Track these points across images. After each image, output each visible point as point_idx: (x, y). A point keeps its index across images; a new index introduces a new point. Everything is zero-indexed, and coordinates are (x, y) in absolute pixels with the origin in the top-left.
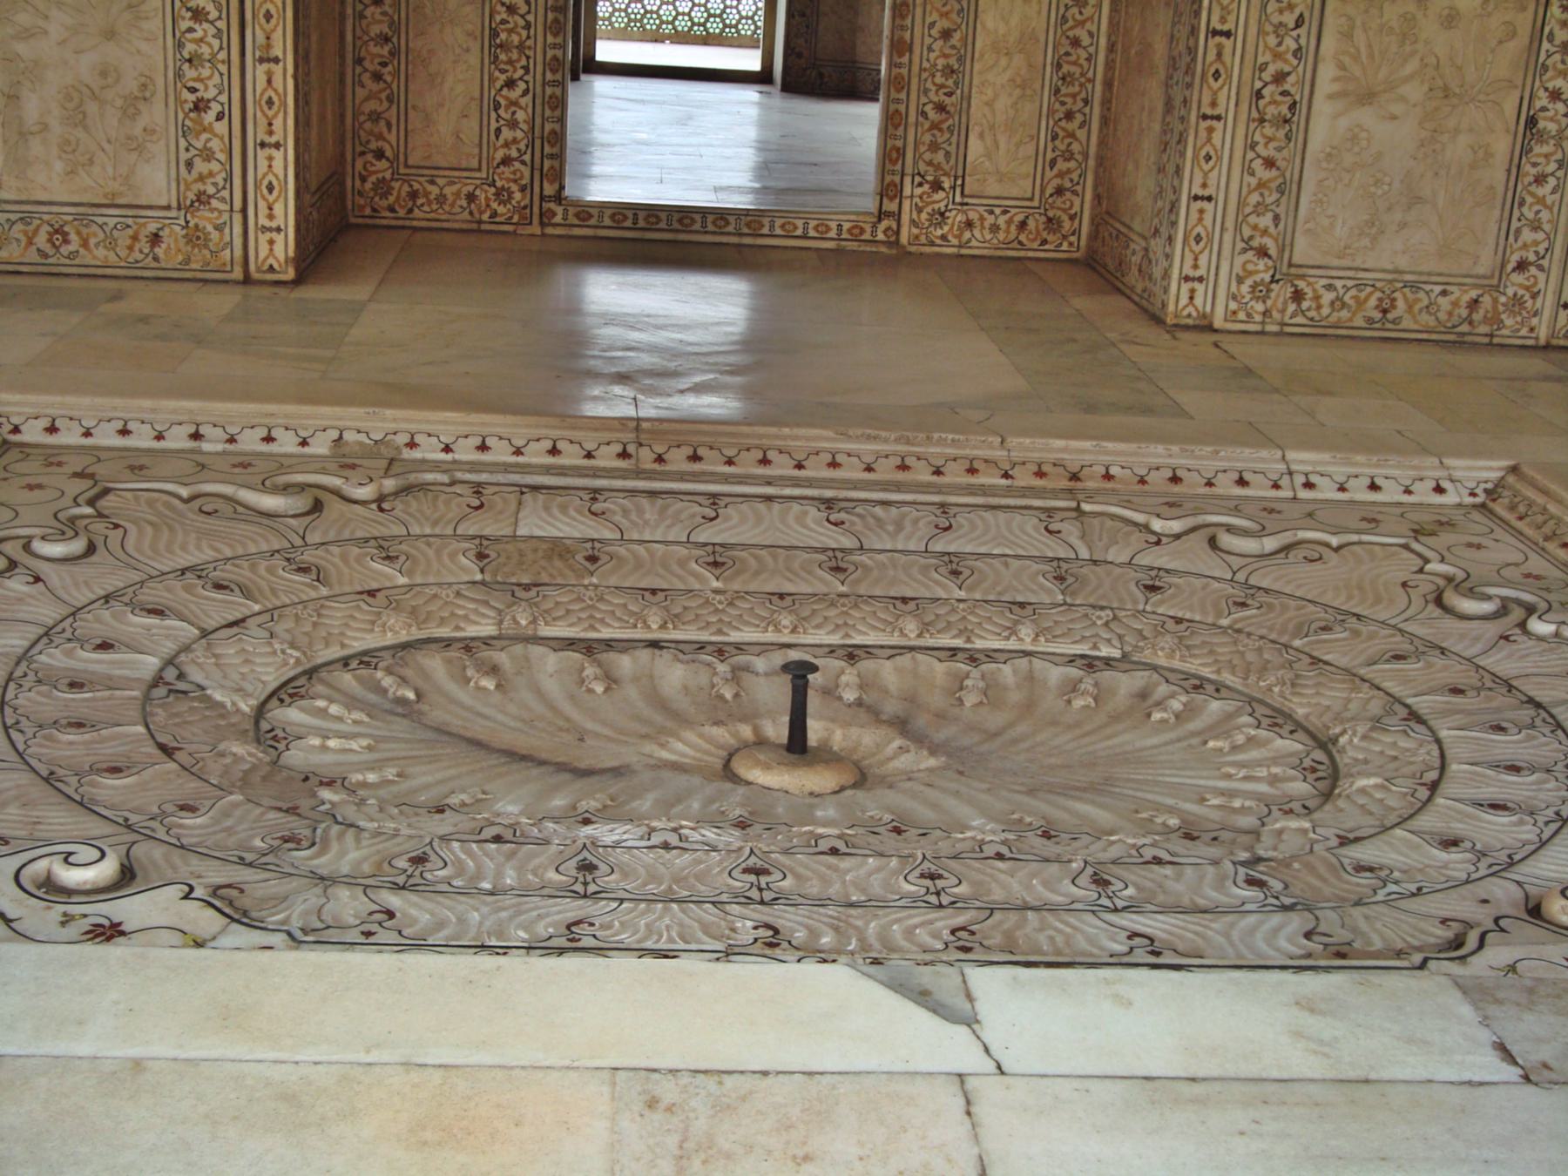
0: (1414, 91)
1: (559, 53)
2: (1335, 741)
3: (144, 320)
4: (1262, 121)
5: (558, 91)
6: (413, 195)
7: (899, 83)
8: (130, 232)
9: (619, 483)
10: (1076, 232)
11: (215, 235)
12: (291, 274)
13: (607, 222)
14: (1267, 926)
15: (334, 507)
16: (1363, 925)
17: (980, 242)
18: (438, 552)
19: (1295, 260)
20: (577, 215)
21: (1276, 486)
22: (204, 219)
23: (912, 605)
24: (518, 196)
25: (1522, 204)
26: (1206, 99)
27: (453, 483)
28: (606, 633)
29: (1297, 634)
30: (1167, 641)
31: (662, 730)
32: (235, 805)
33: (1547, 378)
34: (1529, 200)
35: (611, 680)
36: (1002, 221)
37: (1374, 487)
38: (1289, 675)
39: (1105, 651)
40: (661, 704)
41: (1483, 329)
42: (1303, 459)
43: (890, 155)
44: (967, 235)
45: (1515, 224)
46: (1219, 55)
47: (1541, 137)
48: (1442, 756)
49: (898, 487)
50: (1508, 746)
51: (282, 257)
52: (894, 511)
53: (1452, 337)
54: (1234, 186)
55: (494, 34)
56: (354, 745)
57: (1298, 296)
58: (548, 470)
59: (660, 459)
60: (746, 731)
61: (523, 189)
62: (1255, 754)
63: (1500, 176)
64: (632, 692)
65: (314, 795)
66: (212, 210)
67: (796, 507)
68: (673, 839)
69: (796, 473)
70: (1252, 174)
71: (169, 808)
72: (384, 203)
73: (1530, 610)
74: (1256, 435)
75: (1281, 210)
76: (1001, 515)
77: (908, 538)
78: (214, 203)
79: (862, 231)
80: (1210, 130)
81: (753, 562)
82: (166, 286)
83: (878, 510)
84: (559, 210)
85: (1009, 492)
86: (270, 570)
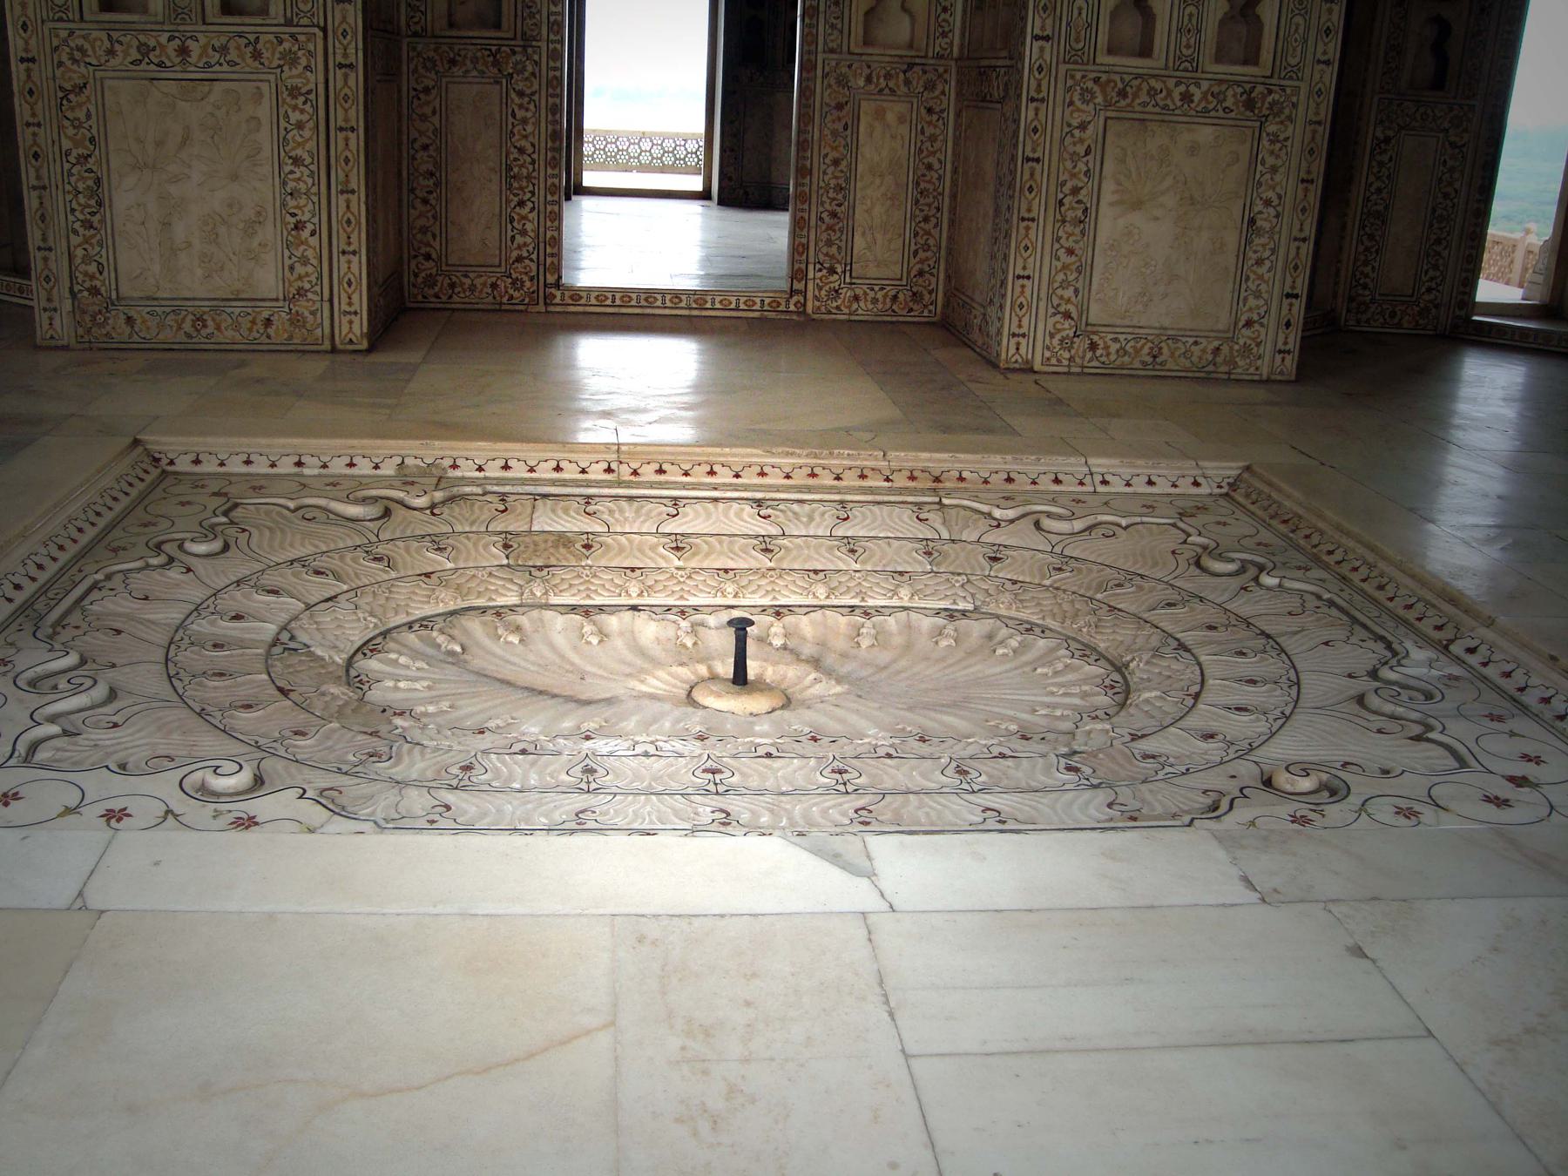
1: (556, 181)
2: (1127, 666)
3: (260, 381)
4: (1064, 221)
5: (556, 208)
7: (803, 198)
9: (606, 491)
10: (934, 303)
12: (365, 345)
13: (593, 302)
14: (1080, 801)
15: (399, 513)
16: (1148, 797)
17: (864, 310)
18: (475, 545)
20: (571, 297)
21: (1081, 484)
22: (303, 307)
23: (821, 575)
24: (528, 284)
25: (1248, 279)
26: (1024, 206)
27: (484, 494)
28: (598, 601)
29: (1099, 589)
30: (1007, 597)
31: (642, 671)
32: (333, 731)
34: (1252, 276)
35: (603, 635)
36: (880, 295)
37: (1150, 483)
38: (1093, 620)
39: (961, 606)
40: (641, 652)
41: (1223, 369)
42: (1100, 464)
43: (798, 249)
44: (855, 306)
46: (1032, 175)
47: (1260, 232)
48: (1202, 674)
49: (810, 489)
50: (1247, 666)
52: (806, 507)
54: (1046, 270)
56: (418, 686)
57: (1093, 346)
58: (553, 483)
59: (635, 473)
60: (703, 670)
61: (532, 279)
62: (1070, 677)
64: (619, 643)
65: (390, 722)
67: (735, 505)
68: (652, 750)
69: (735, 481)
70: (1058, 259)
71: (287, 733)
72: (431, 292)
73: (1261, 568)
74: (1067, 447)
76: (885, 508)
77: (818, 526)
78: (310, 295)
79: (779, 304)
80: (1028, 228)
81: (705, 547)
82: (274, 356)
83: (795, 507)
84: (558, 294)
85: (890, 491)
86: (354, 560)
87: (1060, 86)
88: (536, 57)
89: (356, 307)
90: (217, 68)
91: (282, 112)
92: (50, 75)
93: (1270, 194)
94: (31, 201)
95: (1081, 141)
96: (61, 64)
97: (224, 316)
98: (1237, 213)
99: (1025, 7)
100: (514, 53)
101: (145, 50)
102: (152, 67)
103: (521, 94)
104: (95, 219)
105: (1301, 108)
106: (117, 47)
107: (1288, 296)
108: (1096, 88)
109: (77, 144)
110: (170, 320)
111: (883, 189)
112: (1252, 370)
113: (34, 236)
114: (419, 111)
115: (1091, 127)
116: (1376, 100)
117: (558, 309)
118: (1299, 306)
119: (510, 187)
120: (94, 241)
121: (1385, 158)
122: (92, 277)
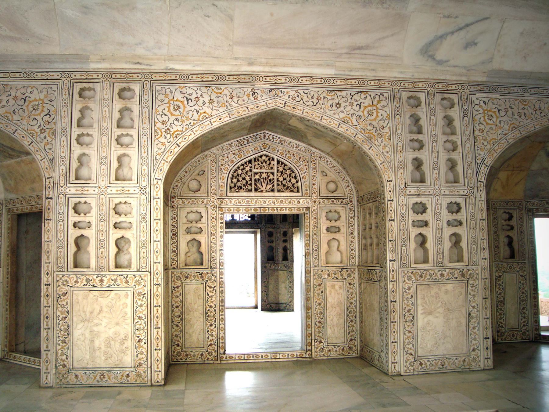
0: (441, 310)
3: (129, 401)
4: (406, 322)
6: (187, 355)
8: (121, 374)
10: (357, 350)
11: (143, 374)
12: (163, 383)
17: (333, 355)
19: (419, 355)
20: (229, 357)
22: (141, 370)
24: (214, 353)
25: (471, 334)
26: (392, 318)
33: (489, 380)
34: (472, 333)
36: (338, 349)
41: (468, 367)
44: (329, 353)
45: (470, 340)
47: (472, 318)
51: (161, 379)
53: (460, 370)
54: (402, 339)
55: (207, 313)
57: (421, 364)
61: (215, 352)
63: (465, 328)
66: (143, 367)
72: (179, 358)
75: (414, 343)
78: (143, 365)
79: (303, 355)
80: (394, 325)
82: (131, 388)
84: (225, 356)
87: (400, 276)
88: (215, 275)
89: (160, 369)
90: (113, 286)
91: (135, 301)
92: (55, 290)
93: (474, 304)
94: (43, 333)
95: (409, 293)
96: (59, 286)
97: (112, 374)
98: (464, 312)
99: (385, 250)
100: (208, 273)
101: (88, 281)
102: (90, 286)
103: (210, 287)
104: (67, 340)
105: (480, 275)
106: (79, 280)
107: (486, 338)
108: (412, 275)
109: (62, 313)
110: (92, 376)
111: (336, 312)
112: (477, 366)
113: (43, 347)
114: (175, 294)
115: (412, 289)
116: (494, 263)
117: (225, 362)
118: (490, 342)
119: (207, 320)
120: (66, 347)
121: (500, 282)
122: (64, 361)
